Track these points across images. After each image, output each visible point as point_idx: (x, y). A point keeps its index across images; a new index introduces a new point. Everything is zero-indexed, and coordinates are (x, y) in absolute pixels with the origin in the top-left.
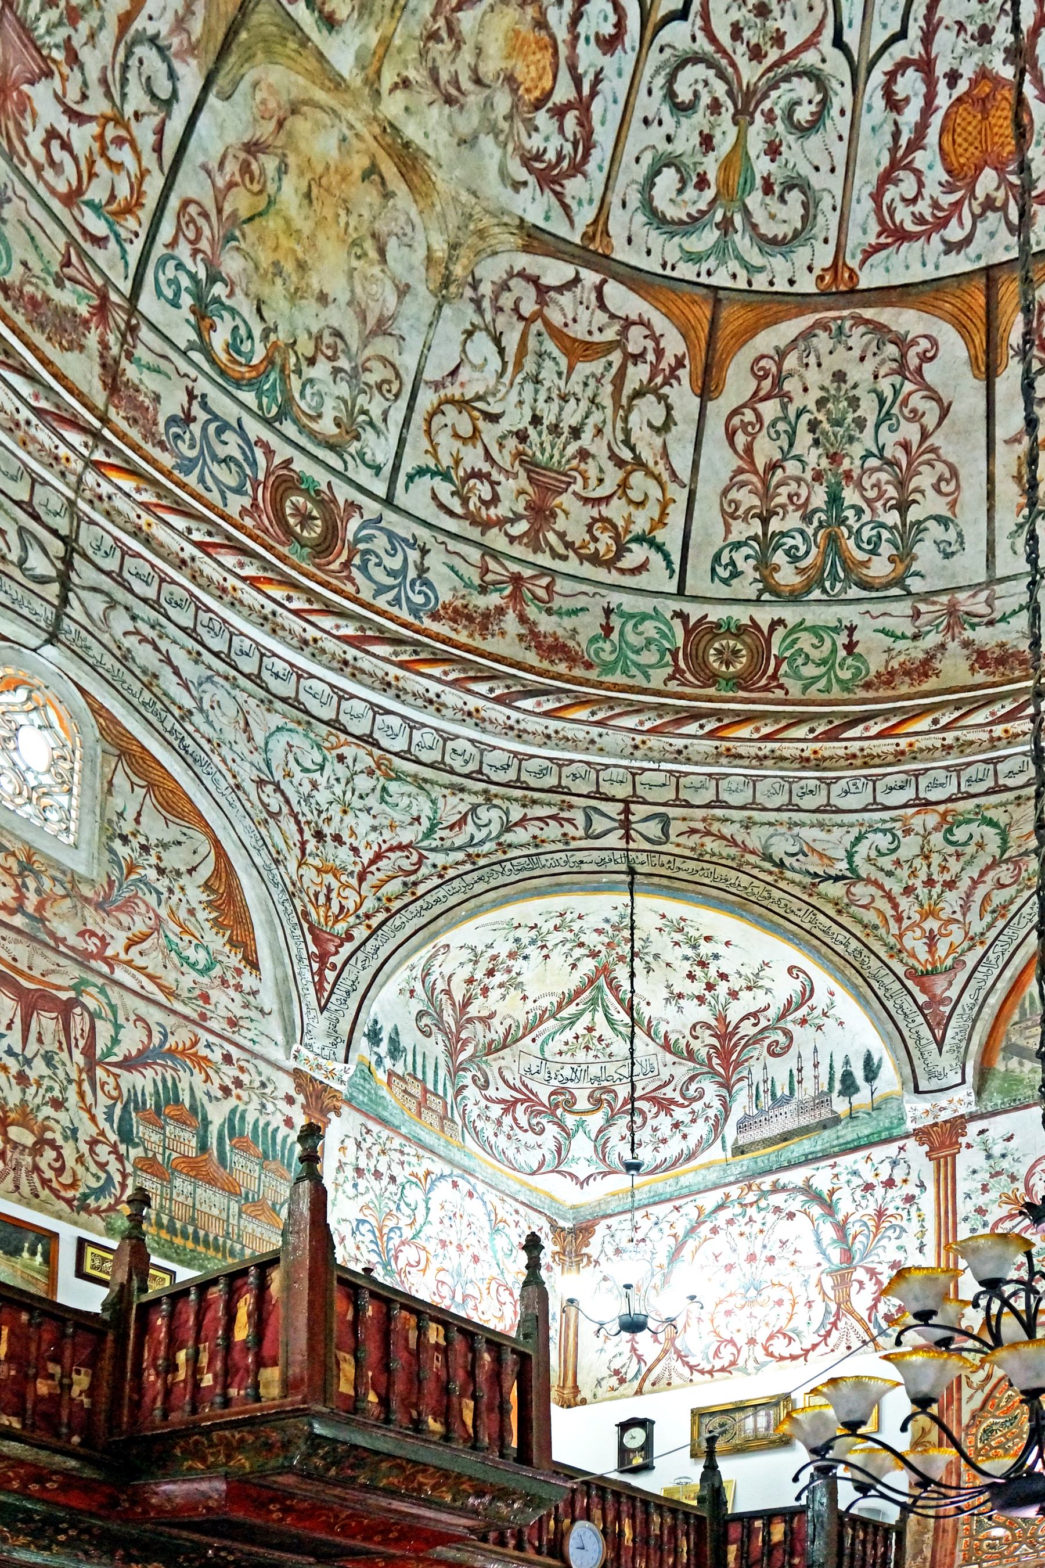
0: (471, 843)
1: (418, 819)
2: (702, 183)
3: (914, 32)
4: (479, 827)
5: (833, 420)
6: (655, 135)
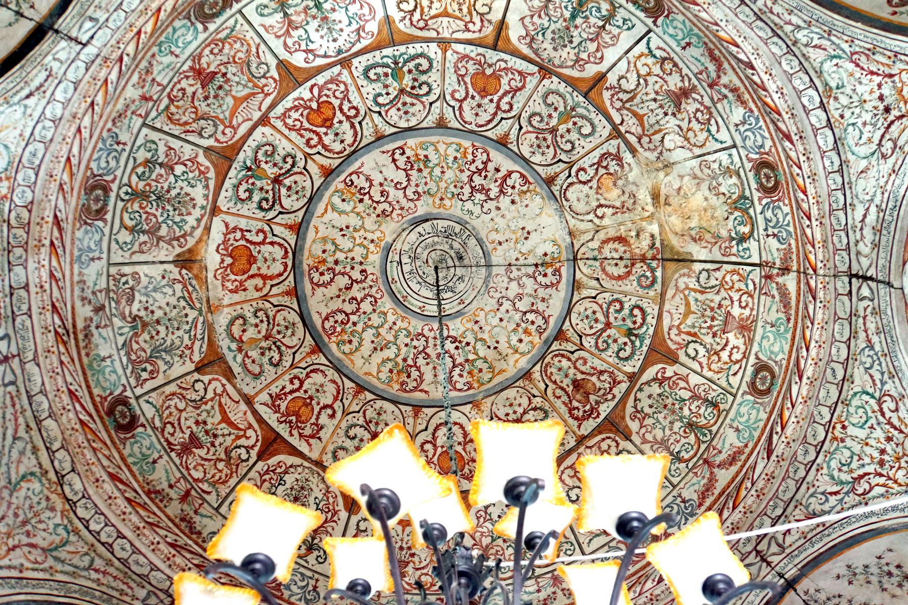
0: (822, 37)
1: (837, 65)
2: (575, 124)
3: (498, 118)
4: (812, 39)
5: (563, 38)
6: (582, 143)
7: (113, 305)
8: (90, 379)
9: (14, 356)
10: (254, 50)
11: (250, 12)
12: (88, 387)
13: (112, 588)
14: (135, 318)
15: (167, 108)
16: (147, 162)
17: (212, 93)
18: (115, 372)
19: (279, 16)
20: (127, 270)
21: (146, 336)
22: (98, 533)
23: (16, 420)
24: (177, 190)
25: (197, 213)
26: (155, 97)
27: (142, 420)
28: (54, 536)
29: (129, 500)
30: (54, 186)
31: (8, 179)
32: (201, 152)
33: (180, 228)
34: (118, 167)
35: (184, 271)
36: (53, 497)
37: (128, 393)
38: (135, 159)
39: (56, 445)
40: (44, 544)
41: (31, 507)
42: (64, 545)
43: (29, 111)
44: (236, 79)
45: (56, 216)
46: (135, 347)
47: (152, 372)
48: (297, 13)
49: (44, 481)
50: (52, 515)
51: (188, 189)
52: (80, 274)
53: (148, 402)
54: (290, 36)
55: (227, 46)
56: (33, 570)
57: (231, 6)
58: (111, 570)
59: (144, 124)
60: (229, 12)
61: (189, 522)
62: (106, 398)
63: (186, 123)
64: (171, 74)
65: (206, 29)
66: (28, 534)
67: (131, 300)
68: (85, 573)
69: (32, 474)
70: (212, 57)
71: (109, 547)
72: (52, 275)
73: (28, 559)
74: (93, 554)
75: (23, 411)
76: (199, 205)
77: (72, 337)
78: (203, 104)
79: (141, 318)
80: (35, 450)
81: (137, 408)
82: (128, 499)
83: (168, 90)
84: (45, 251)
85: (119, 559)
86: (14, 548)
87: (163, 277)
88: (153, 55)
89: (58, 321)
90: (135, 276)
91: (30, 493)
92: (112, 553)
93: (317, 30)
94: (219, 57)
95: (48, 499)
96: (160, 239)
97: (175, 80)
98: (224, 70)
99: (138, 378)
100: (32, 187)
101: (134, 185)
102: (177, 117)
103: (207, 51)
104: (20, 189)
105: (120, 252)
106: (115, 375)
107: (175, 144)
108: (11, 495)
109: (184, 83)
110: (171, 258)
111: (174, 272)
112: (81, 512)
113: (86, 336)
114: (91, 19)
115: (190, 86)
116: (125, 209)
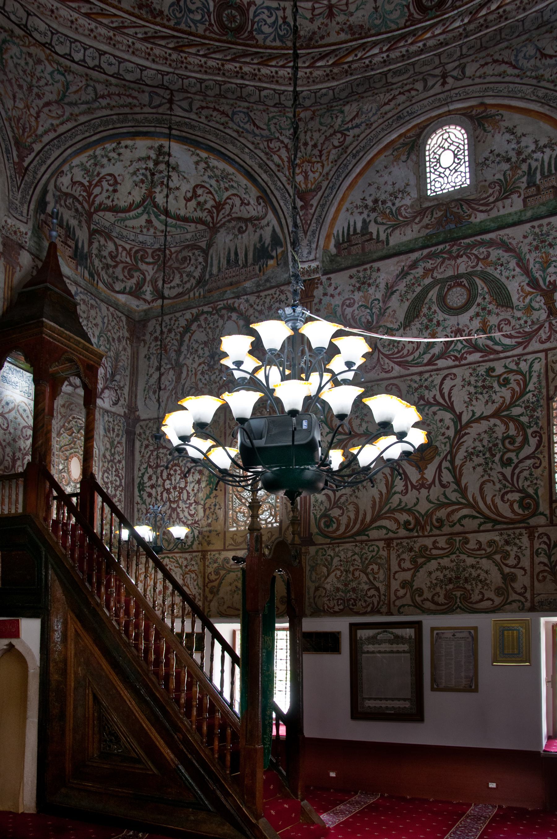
13: (123, 106)
42: (68, 89)
49: (17, 41)
50: (42, 67)
56: (62, 123)
58: (113, 89)
61: (147, 6)
66: (38, 96)
68: (96, 105)
73: (52, 117)
85: (112, 76)
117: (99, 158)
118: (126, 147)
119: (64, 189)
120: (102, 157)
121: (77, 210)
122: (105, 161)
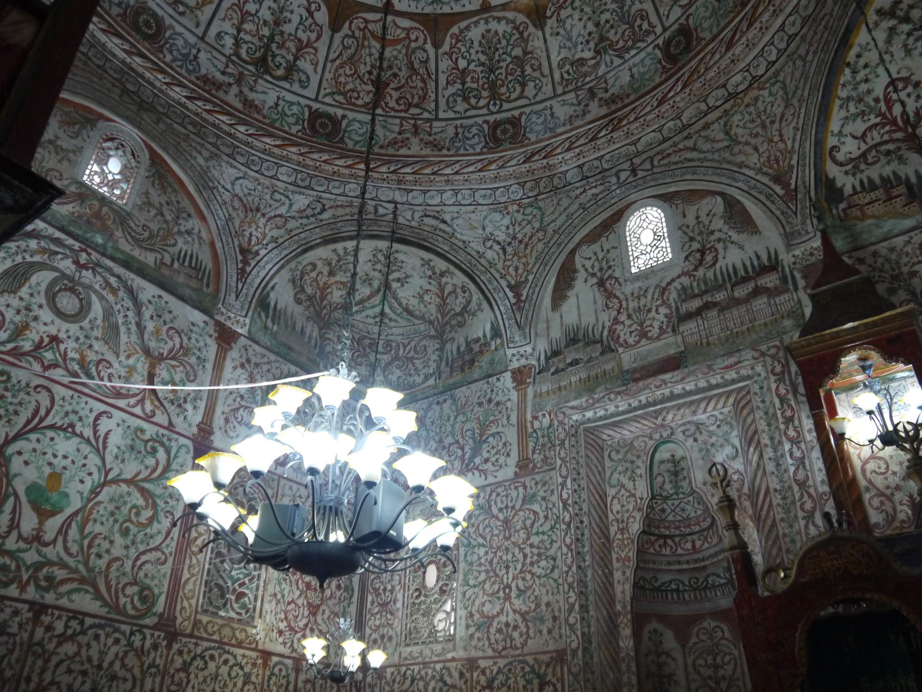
7: (588, 79)
8: (647, 89)
9: (632, 164)
10: (338, 62)
11: (311, 92)
12: (654, 89)
14: (597, 52)
15: (417, 106)
16: (466, 99)
17: (389, 73)
18: (642, 61)
19: (301, 64)
20: (557, 76)
21: (611, 35)
22: (779, 51)
23: (681, 150)
24: (480, 55)
25: (493, 25)
26: (412, 122)
27: (682, 21)
28: (778, 96)
29: (750, 25)
30: (503, 172)
31: (506, 208)
32: (440, 51)
33: (511, 35)
34: (476, 124)
35: (548, 13)
36: (747, 100)
37: (660, 41)
38: (466, 111)
39: (703, 107)
40: (783, 105)
41: (753, 121)
43: (455, 215)
44: (368, 59)
45: (524, 162)
46: (621, 44)
47: (642, 20)
48: (288, 49)
51: (476, 44)
52: (564, 125)
53: (668, 16)
54: (309, 39)
55: (348, 88)
57: (317, 110)
59: (437, 119)
60: (323, 108)
62: (664, 67)
63: (423, 81)
64: (390, 120)
65: (344, 117)
66: (772, 122)
67: (582, 61)
69: (725, 125)
70: (361, 95)
71: (791, 38)
72: (569, 149)
74: (796, 56)
75: (675, 144)
76: (486, 27)
77: (617, 109)
78: (401, 74)
79: (596, 45)
80: (707, 126)
81: (672, 29)
82: (748, 28)
83: (403, 114)
84: (553, 161)
86: (781, 135)
87: (558, 34)
88: (381, 147)
89: (602, 134)
90: (561, 66)
91: (741, 124)
92: (796, 35)
93: (290, 21)
94: (359, 88)
95: (748, 106)
96: (525, 53)
97: (392, 114)
98: (367, 76)
99: (648, 33)
100: (507, 188)
101: (486, 101)
102: (420, 92)
103: (360, 102)
104: (512, 196)
105: (544, 89)
106: (643, 59)
107: (442, 79)
108: (739, 143)
109: (392, 104)
110: (540, 33)
111: (551, 23)
112: (760, 73)
113: (613, 102)
114: (376, 211)
115: (392, 97)
116: (508, 101)
117: (854, 94)
118: (859, 56)
119: (856, 154)
120: (855, 89)
121: (888, 153)
122: (863, 87)
